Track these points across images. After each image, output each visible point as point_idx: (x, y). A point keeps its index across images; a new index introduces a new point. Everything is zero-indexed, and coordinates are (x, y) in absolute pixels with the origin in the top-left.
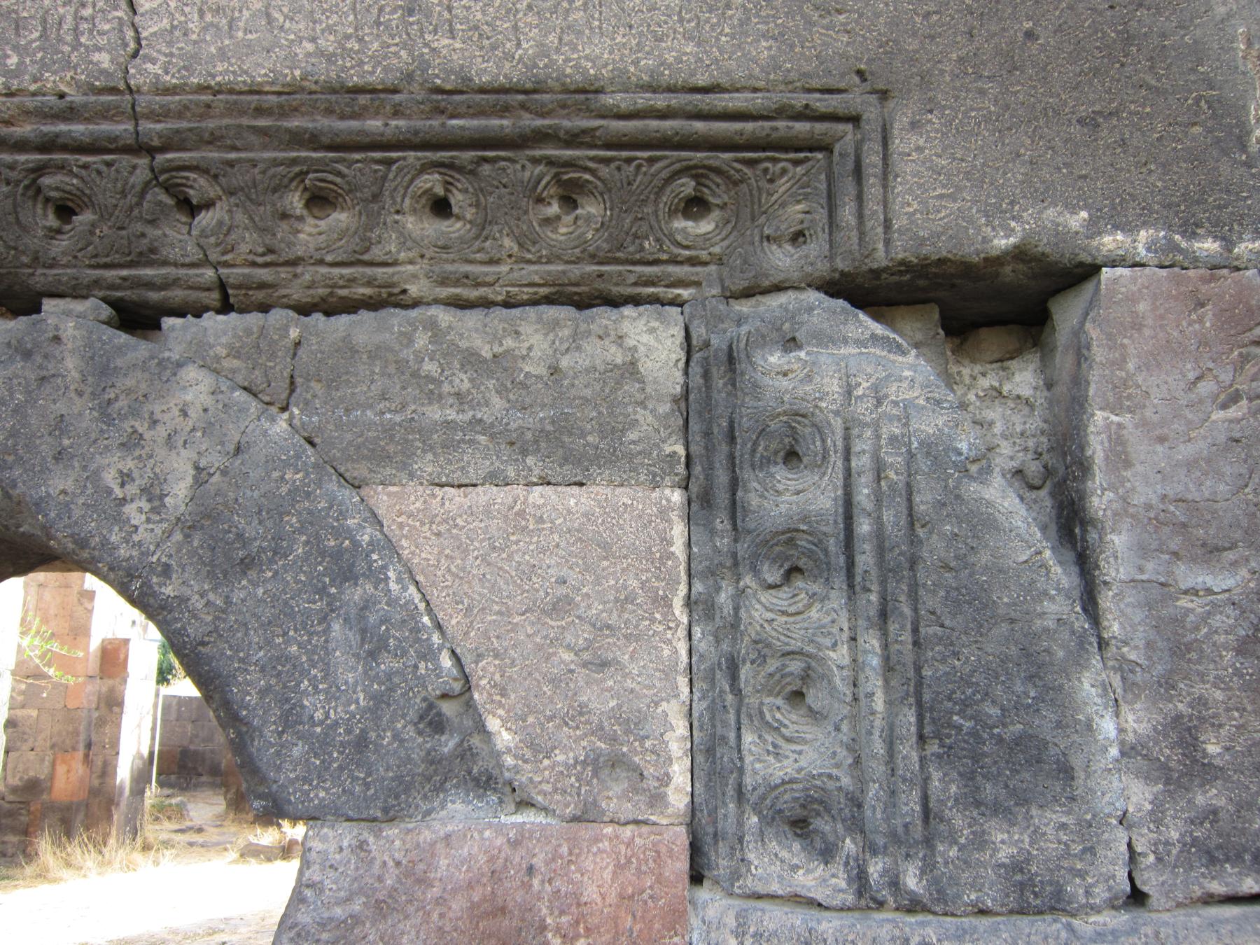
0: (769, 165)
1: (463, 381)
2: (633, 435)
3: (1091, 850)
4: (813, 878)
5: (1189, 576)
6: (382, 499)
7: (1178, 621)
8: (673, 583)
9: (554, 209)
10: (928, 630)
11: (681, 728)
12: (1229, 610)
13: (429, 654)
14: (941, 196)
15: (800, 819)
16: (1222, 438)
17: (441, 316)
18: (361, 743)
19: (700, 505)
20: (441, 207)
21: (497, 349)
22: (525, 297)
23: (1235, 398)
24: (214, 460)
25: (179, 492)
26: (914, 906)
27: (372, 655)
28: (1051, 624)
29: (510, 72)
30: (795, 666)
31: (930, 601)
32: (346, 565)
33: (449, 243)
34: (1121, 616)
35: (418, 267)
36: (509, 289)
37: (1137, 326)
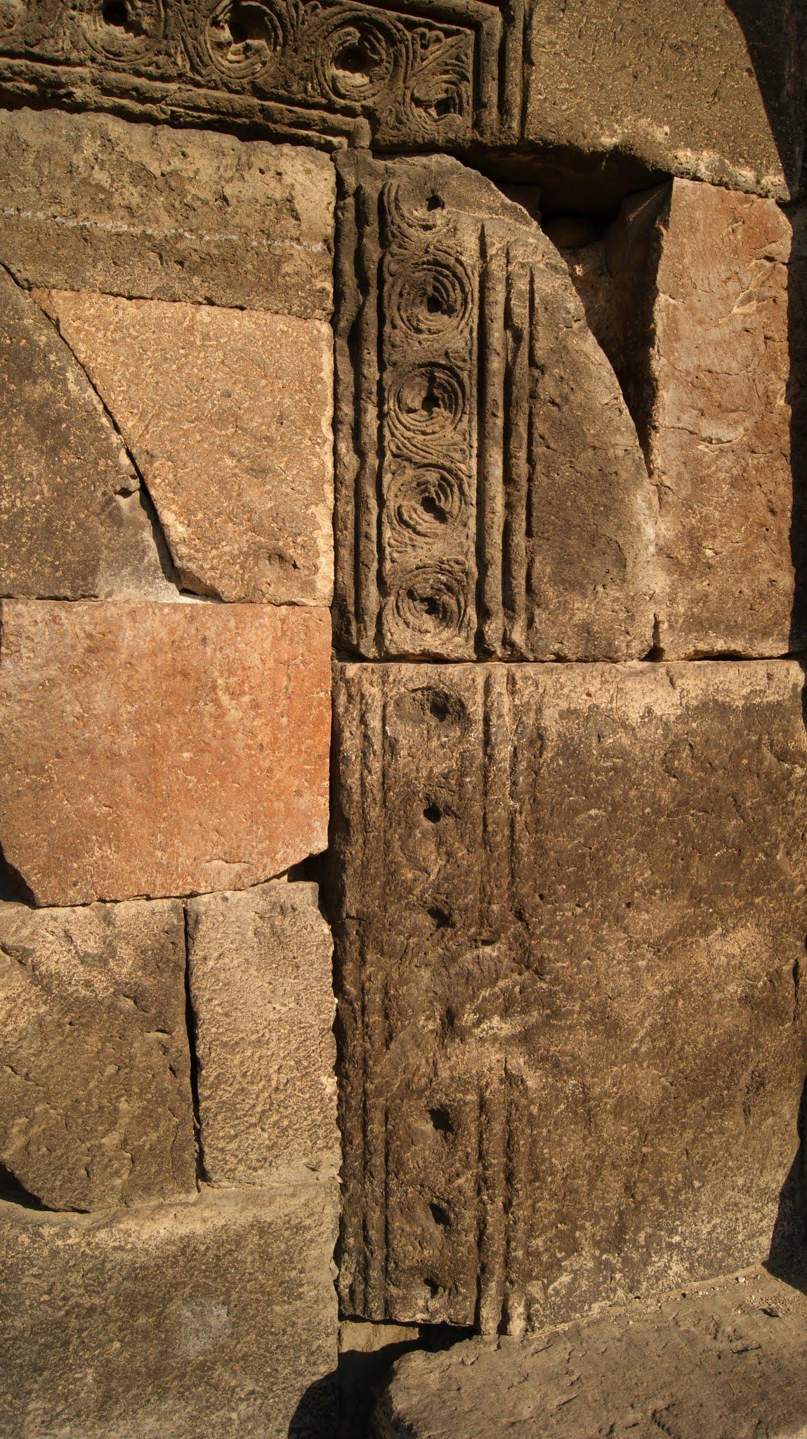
0: (426, 30)
1: (133, 195)
2: (287, 268)
3: (632, 618)
4: (436, 638)
5: (709, 428)
7: (698, 460)
8: (321, 404)
9: (226, 34)
10: (539, 450)
11: (327, 528)
12: (730, 455)
13: (108, 453)
14: (566, 90)
16: (739, 327)
17: (110, 126)
19: (352, 340)
21: (167, 169)
22: (189, 119)
23: (749, 299)
27: (53, 450)
28: (620, 453)
30: (433, 476)
31: (541, 427)
32: (24, 363)
33: (123, 50)
35: (87, 70)
36: (175, 109)
37: (693, 229)
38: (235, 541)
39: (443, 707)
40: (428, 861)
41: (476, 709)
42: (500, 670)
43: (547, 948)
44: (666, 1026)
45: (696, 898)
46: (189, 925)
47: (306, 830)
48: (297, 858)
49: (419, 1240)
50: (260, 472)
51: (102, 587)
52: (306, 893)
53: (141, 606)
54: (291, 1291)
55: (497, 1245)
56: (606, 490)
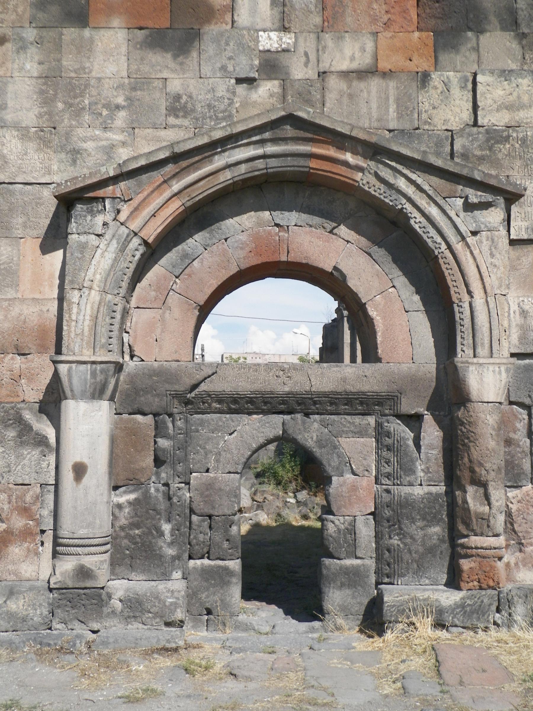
1: (348, 425)
4: (388, 482)
6: (340, 439)
15: (388, 476)
18: (337, 468)
19: (377, 441)
20: (346, 404)
24: (319, 434)
25: (315, 438)
26: (398, 485)
29: (355, 390)
32: (335, 447)
34: (422, 456)
38: (362, 468)
39: (388, 491)
40: (387, 513)
41: (392, 492)
42: (395, 487)
43: (403, 526)
44: (423, 541)
45: (428, 521)
46: (355, 520)
47: (371, 508)
48: (369, 512)
49: (386, 569)
50: (365, 459)
51: (344, 475)
52: (371, 517)
53: (349, 476)
54: (368, 577)
55: (396, 571)
56: (413, 461)
